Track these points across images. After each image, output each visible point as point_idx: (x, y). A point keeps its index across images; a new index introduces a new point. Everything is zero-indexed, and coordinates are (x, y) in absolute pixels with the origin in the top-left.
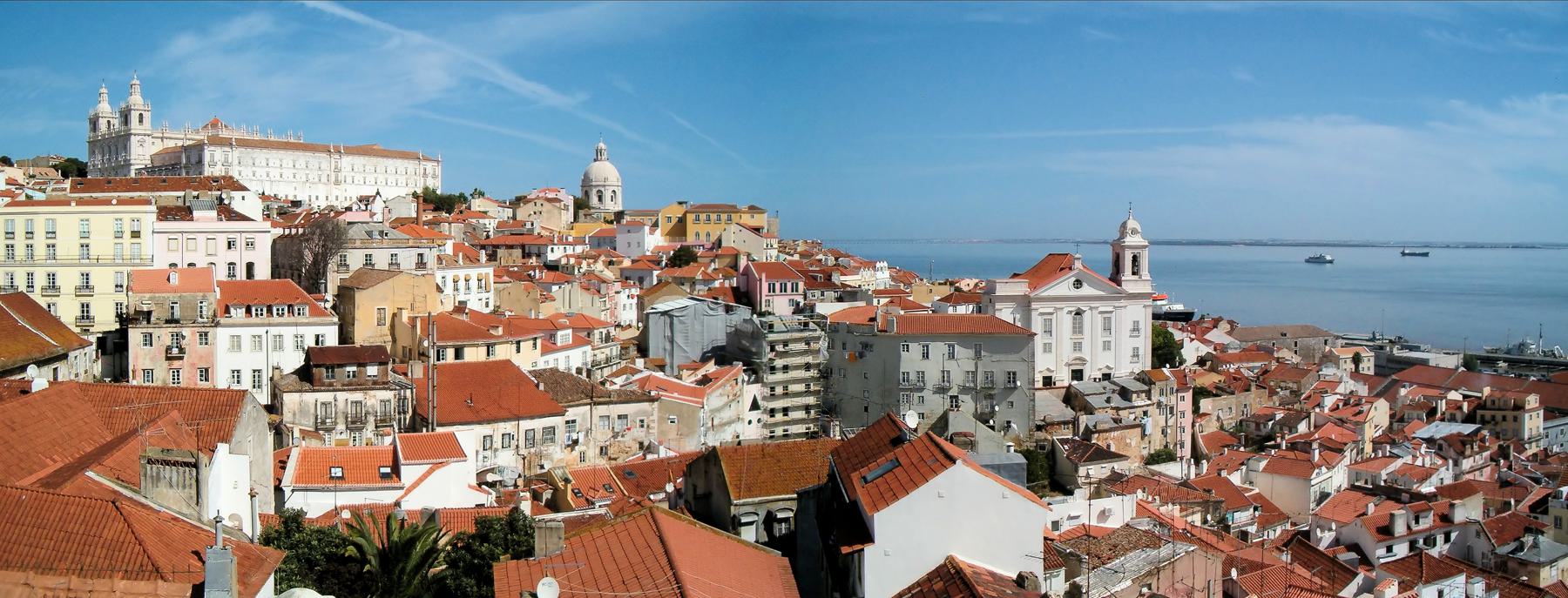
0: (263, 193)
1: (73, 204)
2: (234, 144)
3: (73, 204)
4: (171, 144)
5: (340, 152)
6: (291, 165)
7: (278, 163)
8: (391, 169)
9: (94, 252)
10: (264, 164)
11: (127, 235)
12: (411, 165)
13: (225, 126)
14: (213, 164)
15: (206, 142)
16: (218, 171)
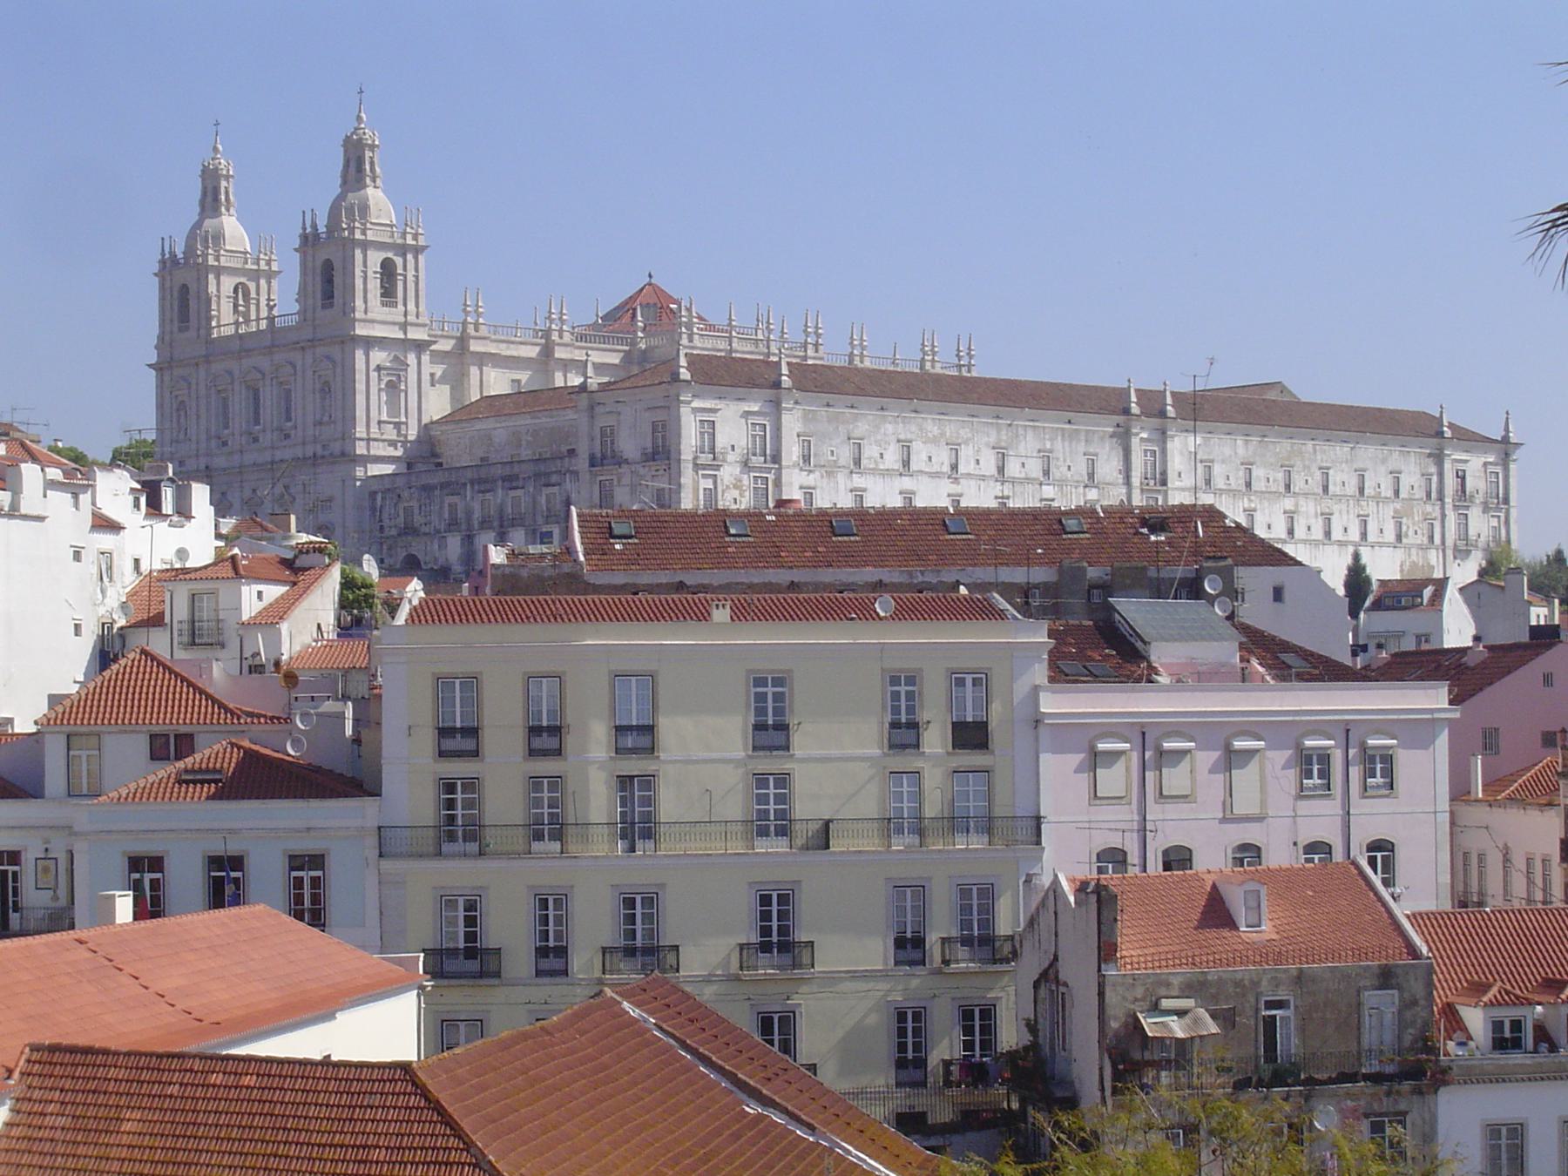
0: (1357, 580)
1: (721, 615)
2: (786, 381)
3: (721, 615)
4: (498, 382)
5: (1162, 414)
6: (989, 465)
7: (943, 458)
8: (1343, 479)
9: (807, 807)
10: (892, 459)
11: (936, 739)
12: (1411, 467)
13: (700, 318)
14: (711, 458)
15: (685, 374)
16: (735, 492)
